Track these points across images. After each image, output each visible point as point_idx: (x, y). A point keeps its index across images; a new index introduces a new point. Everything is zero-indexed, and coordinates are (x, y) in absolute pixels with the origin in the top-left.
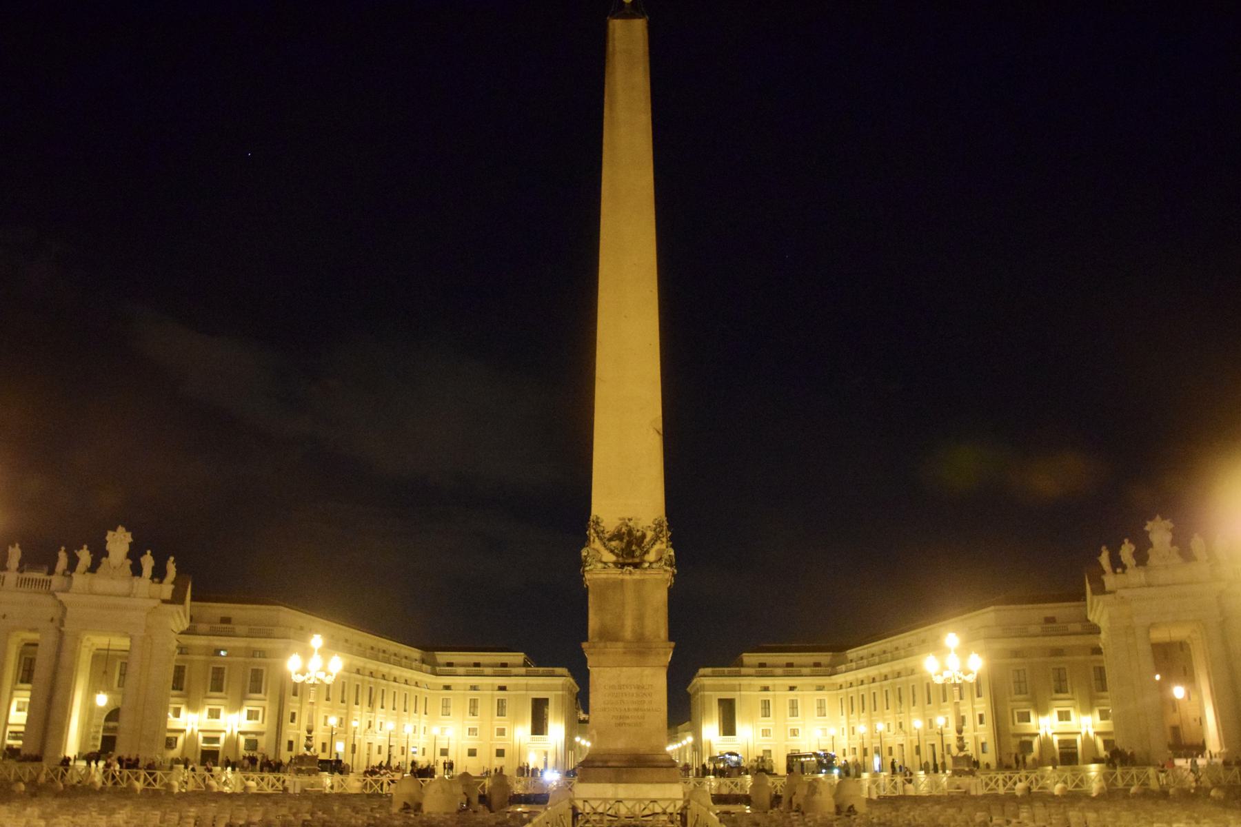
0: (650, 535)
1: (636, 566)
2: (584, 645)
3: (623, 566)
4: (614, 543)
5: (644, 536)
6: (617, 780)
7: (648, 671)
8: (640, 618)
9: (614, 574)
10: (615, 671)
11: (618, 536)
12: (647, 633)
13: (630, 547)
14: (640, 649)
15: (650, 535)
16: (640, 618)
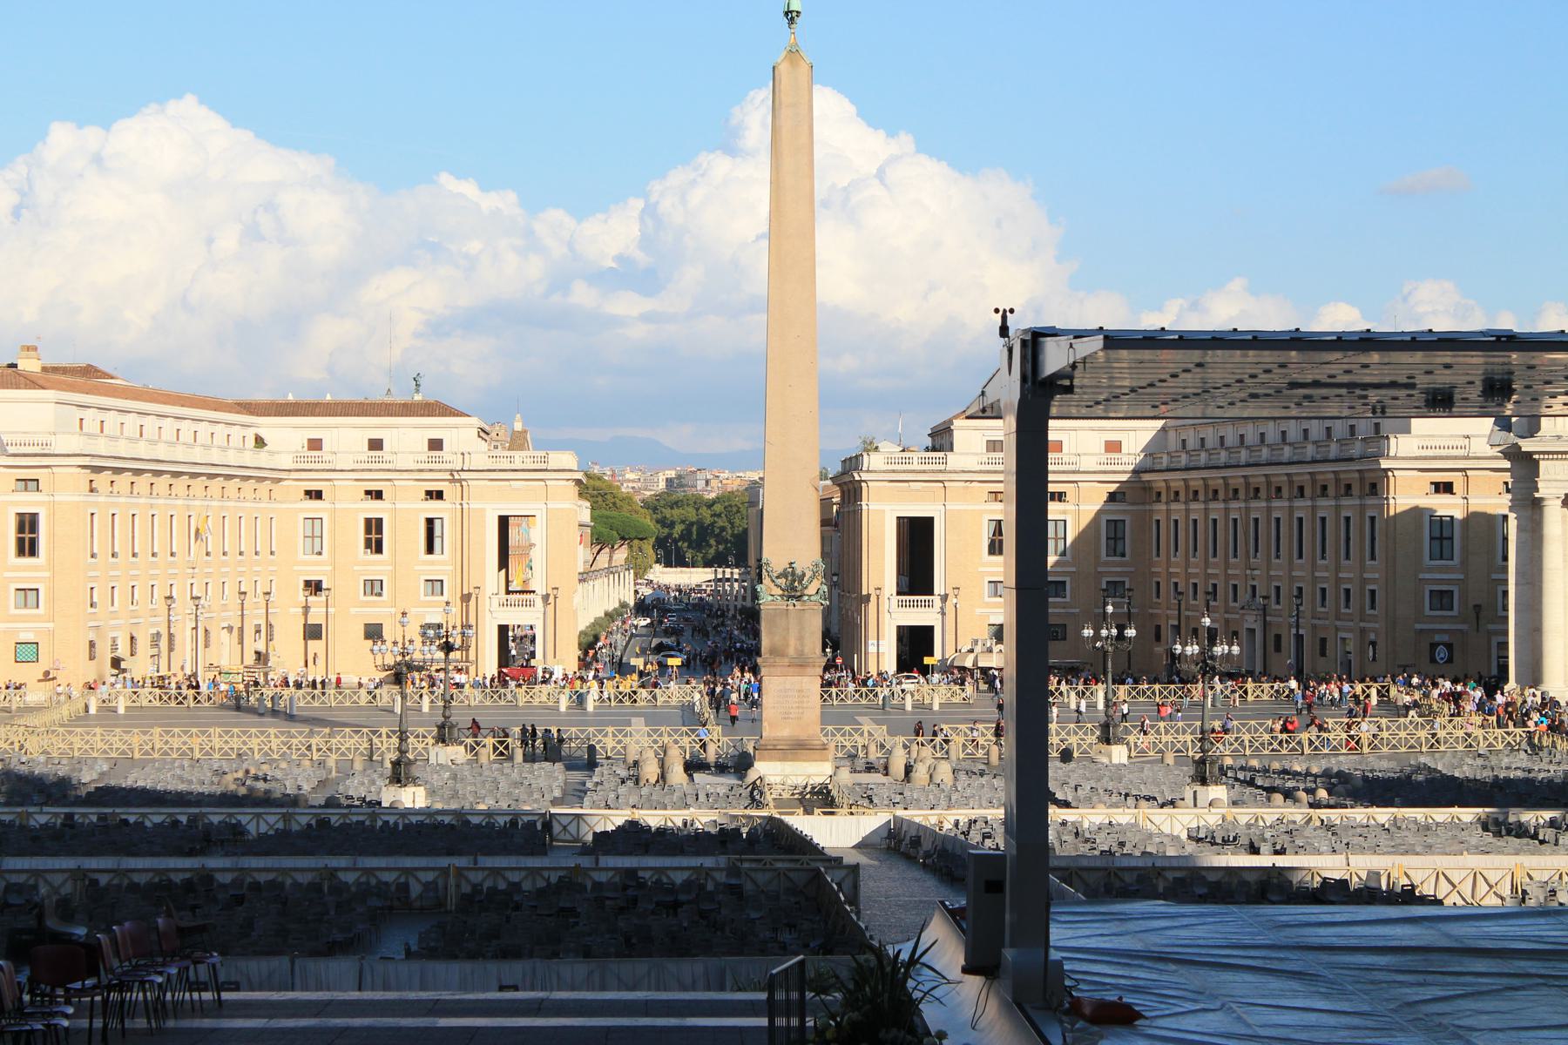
0: (809, 574)
1: (799, 598)
2: (759, 660)
3: (790, 597)
4: (779, 581)
5: (804, 575)
6: (783, 759)
7: (806, 679)
8: (801, 638)
9: (782, 604)
10: (781, 679)
11: (784, 575)
12: (806, 650)
13: (793, 588)
14: (801, 664)
15: (809, 574)
16: (801, 638)
